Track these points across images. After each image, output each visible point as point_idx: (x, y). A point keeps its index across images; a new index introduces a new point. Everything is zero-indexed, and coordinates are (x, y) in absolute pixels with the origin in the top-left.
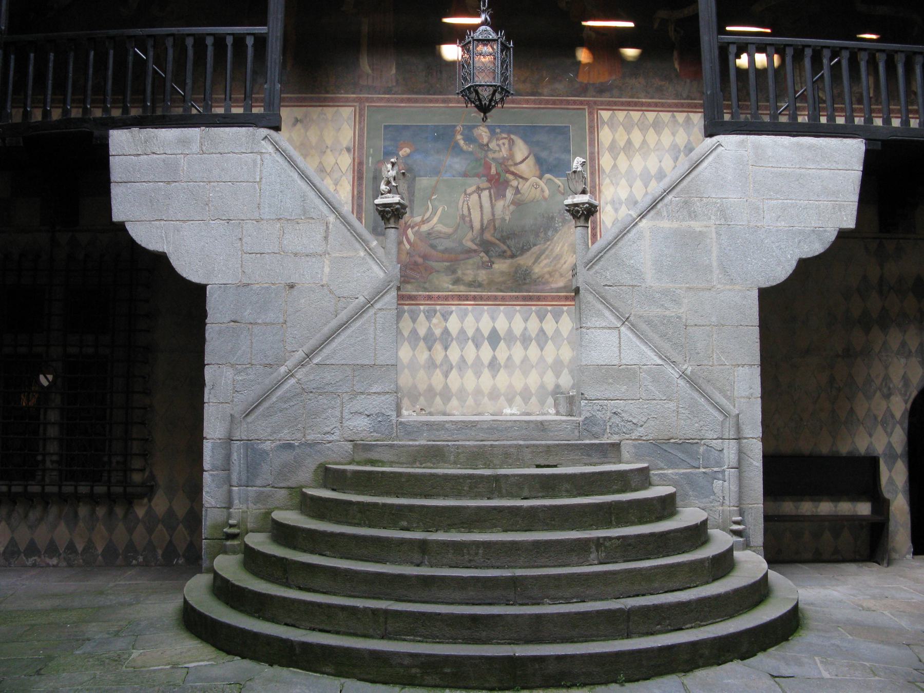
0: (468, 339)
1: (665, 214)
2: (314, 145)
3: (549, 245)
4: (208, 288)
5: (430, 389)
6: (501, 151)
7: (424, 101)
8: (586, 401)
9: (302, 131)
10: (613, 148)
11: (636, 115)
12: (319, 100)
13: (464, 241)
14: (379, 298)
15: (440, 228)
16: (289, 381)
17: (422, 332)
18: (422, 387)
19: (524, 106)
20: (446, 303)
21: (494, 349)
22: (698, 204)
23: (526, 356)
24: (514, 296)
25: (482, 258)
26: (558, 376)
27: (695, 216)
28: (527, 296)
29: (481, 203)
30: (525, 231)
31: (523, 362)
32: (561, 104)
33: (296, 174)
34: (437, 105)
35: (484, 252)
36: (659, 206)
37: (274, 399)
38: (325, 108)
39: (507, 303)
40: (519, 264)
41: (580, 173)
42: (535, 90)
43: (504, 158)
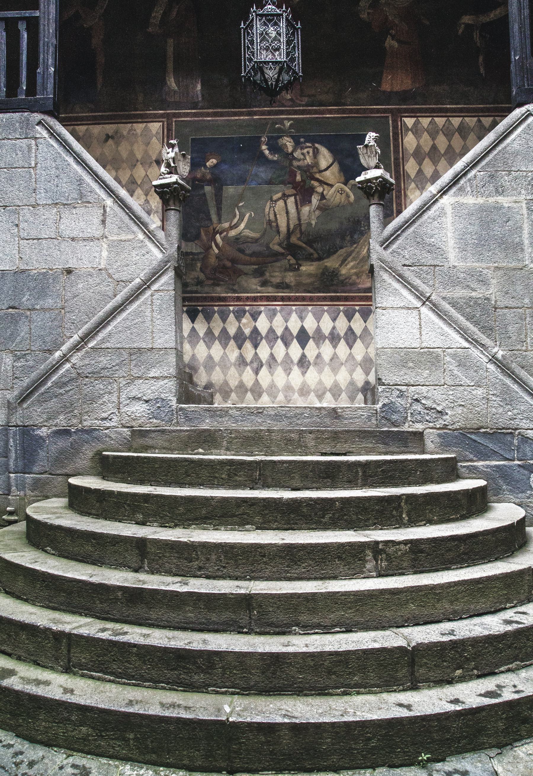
8: (384, 387)
13: (271, 246)
14: (156, 279)
15: (247, 233)
24: (321, 296)
25: (289, 260)
28: (335, 296)
29: (287, 209)
39: (315, 303)
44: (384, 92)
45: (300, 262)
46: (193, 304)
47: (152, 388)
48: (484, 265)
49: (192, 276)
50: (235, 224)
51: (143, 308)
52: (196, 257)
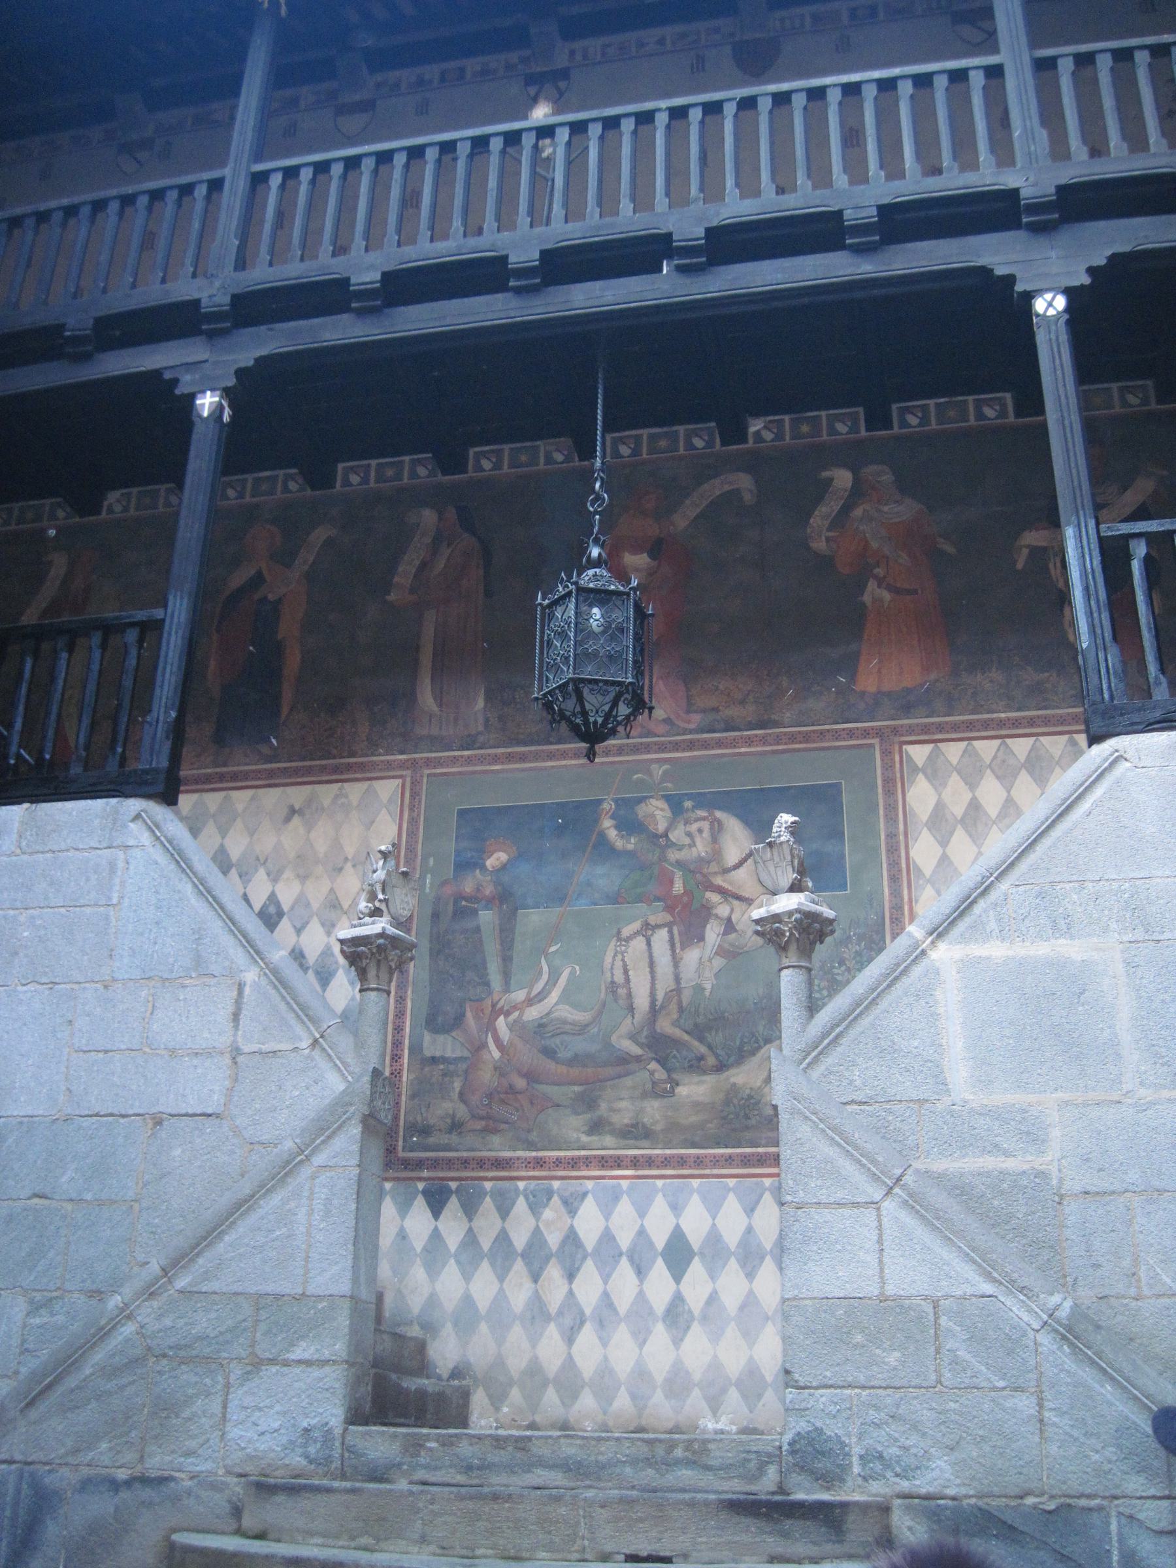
0: (621, 1254)
1: (993, 925)
2: (321, 855)
5: (534, 1370)
6: (695, 845)
7: (537, 757)
9: (302, 831)
10: (939, 821)
11: (987, 748)
12: (336, 770)
13: (614, 1039)
15: (566, 1012)
17: (520, 1239)
19: (743, 750)
21: (678, 1278)
22: (1075, 897)
23: (751, 1293)
25: (652, 1073)
29: (651, 956)
30: (748, 1012)
31: (742, 1307)
32: (822, 741)
33: (189, 886)
34: (564, 763)
35: (658, 1061)
36: (978, 909)
38: (346, 785)
39: (707, 1172)
40: (734, 1084)
41: (785, 846)
42: (766, 717)
43: (701, 860)
44: (863, 694)
45: (675, 1076)
46: (441, 1174)
49: (439, 1112)
50: (539, 993)
51: (293, 1204)
52: (452, 1067)
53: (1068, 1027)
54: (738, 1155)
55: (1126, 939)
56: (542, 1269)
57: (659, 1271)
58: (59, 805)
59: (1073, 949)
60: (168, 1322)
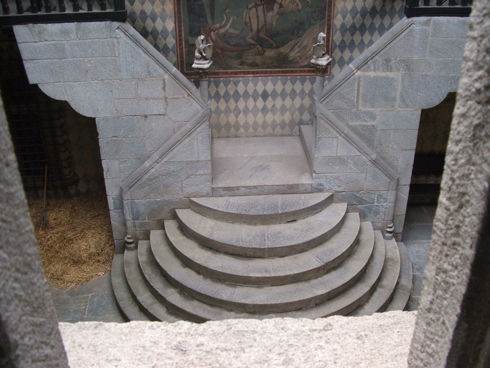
0: (250, 96)
1: (372, 67)
3: (300, 40)
4: (97, 119)
13: (247, 39)
14: (199, 126)
15: (232, 31)
16: (151, 170)
18: (223, 123)
20: (236, 76)
21: (265, 101)
23: (283, 104)
26: (301, 114)
27: (391, 69)
29: (257, 14)
35: (260, 45)
36: (369, 63)
37: (144, 180)
39: (273, 75)
47: (199, 179)
48: (374, 109)
50: (224, 25)
51: (192, 141)
53: (385, 93)
54: (281, 70)
55: (403, 73)
56: (229, 100)
57: (260, 100)
58: (88, 23)
59: (390, 75)
60: (163, 168)
